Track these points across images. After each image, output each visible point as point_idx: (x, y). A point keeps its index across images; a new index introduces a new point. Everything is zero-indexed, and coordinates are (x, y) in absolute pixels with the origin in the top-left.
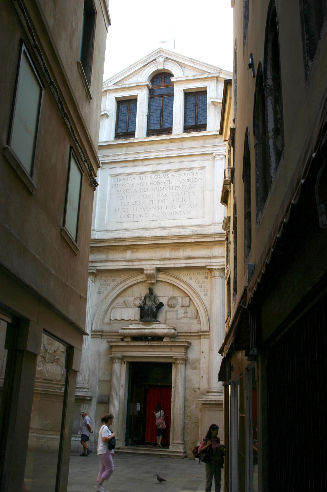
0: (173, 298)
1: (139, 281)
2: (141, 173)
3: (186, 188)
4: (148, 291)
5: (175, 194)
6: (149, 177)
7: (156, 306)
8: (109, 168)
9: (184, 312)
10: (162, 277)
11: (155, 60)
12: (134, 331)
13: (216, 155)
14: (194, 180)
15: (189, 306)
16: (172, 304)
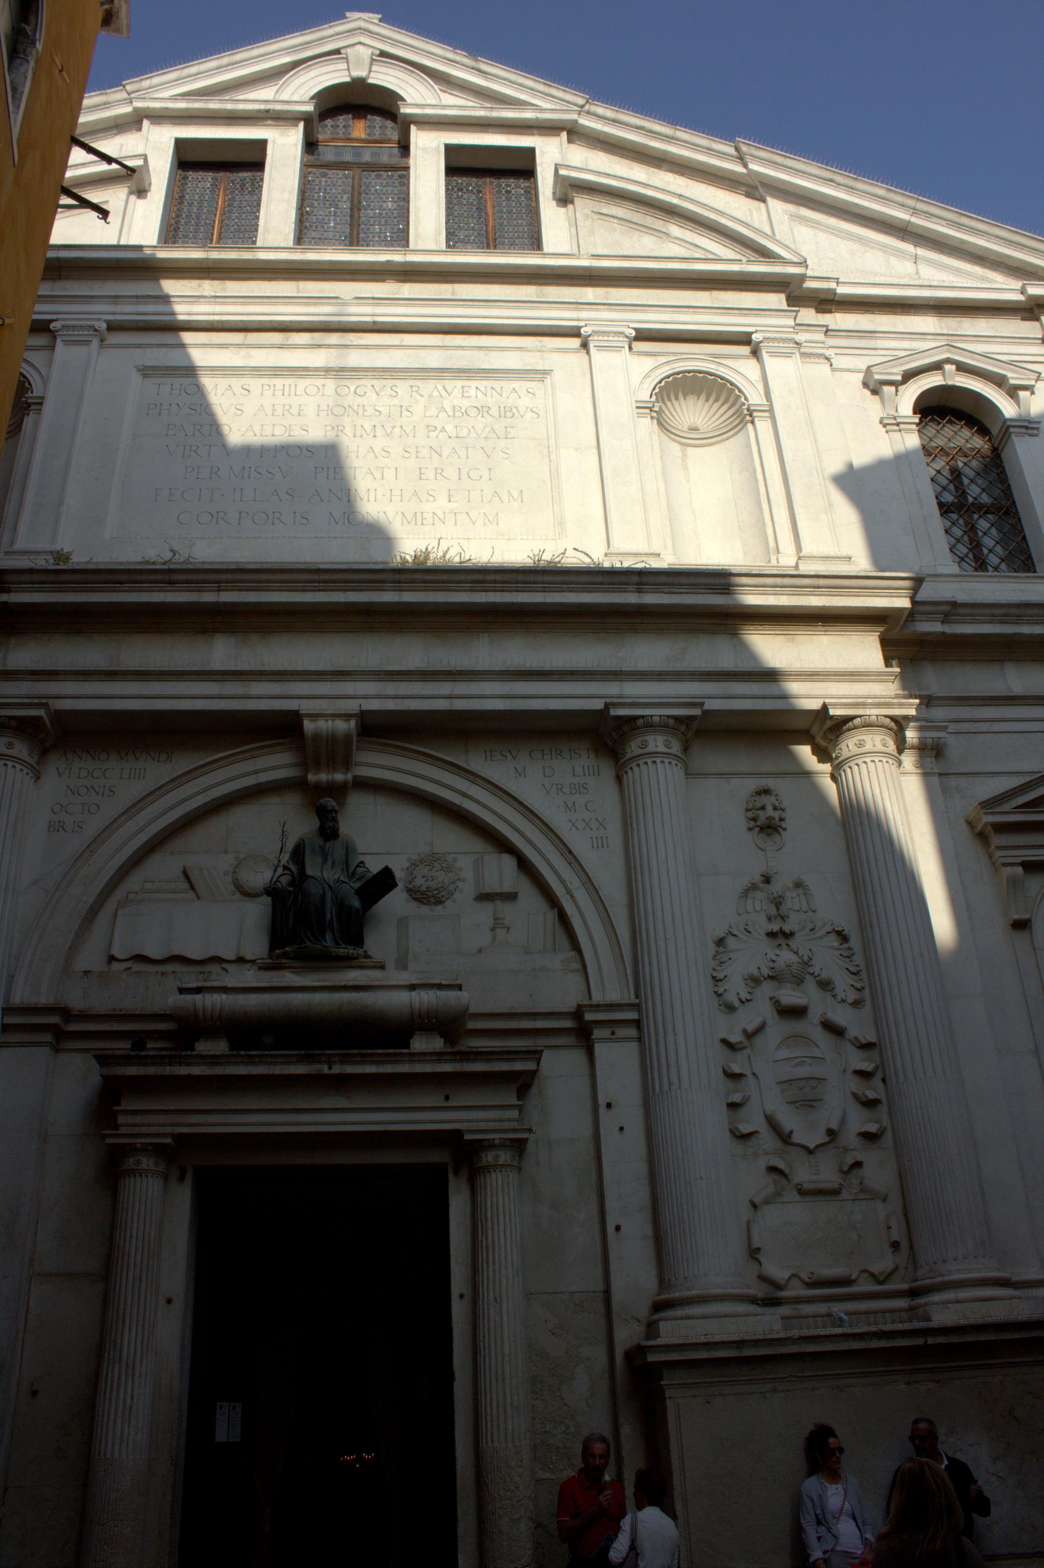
0: (432, 859)
1: (264, 778)
2: (277, 372)
3: (473, 434)
4: (314, 823)
5: (425, 452)
6: (312, 390)
7: (357, 885)
8: (139, 346)
9: (490, 922)
10: (377, 763)
11: (337, 52)
12: (252, 1001)
13: (595, 332)
14: (507, 412)
15: (511, 897)
16: (433, 884)
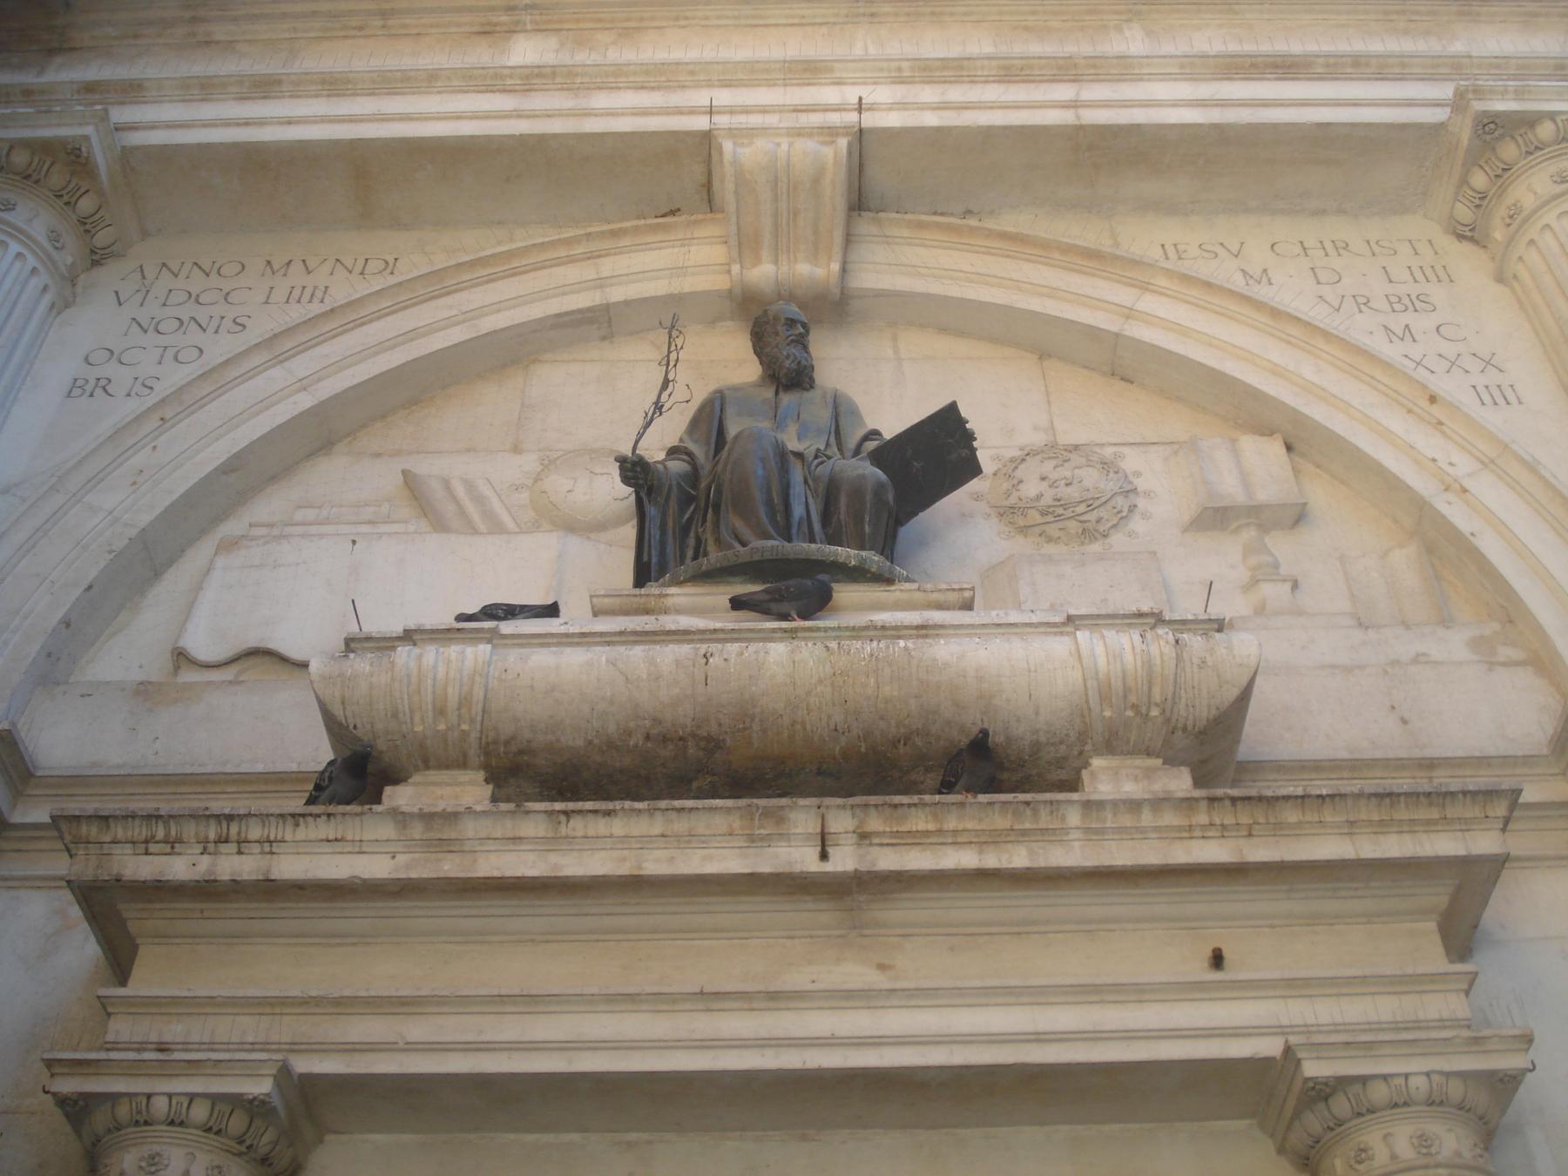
16: (1072, 493)
